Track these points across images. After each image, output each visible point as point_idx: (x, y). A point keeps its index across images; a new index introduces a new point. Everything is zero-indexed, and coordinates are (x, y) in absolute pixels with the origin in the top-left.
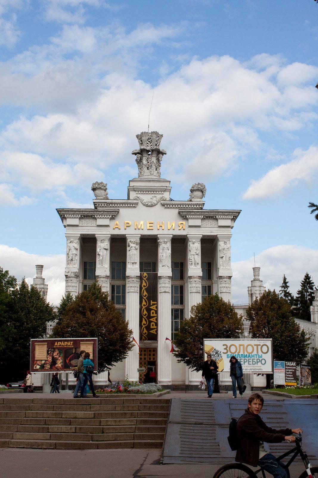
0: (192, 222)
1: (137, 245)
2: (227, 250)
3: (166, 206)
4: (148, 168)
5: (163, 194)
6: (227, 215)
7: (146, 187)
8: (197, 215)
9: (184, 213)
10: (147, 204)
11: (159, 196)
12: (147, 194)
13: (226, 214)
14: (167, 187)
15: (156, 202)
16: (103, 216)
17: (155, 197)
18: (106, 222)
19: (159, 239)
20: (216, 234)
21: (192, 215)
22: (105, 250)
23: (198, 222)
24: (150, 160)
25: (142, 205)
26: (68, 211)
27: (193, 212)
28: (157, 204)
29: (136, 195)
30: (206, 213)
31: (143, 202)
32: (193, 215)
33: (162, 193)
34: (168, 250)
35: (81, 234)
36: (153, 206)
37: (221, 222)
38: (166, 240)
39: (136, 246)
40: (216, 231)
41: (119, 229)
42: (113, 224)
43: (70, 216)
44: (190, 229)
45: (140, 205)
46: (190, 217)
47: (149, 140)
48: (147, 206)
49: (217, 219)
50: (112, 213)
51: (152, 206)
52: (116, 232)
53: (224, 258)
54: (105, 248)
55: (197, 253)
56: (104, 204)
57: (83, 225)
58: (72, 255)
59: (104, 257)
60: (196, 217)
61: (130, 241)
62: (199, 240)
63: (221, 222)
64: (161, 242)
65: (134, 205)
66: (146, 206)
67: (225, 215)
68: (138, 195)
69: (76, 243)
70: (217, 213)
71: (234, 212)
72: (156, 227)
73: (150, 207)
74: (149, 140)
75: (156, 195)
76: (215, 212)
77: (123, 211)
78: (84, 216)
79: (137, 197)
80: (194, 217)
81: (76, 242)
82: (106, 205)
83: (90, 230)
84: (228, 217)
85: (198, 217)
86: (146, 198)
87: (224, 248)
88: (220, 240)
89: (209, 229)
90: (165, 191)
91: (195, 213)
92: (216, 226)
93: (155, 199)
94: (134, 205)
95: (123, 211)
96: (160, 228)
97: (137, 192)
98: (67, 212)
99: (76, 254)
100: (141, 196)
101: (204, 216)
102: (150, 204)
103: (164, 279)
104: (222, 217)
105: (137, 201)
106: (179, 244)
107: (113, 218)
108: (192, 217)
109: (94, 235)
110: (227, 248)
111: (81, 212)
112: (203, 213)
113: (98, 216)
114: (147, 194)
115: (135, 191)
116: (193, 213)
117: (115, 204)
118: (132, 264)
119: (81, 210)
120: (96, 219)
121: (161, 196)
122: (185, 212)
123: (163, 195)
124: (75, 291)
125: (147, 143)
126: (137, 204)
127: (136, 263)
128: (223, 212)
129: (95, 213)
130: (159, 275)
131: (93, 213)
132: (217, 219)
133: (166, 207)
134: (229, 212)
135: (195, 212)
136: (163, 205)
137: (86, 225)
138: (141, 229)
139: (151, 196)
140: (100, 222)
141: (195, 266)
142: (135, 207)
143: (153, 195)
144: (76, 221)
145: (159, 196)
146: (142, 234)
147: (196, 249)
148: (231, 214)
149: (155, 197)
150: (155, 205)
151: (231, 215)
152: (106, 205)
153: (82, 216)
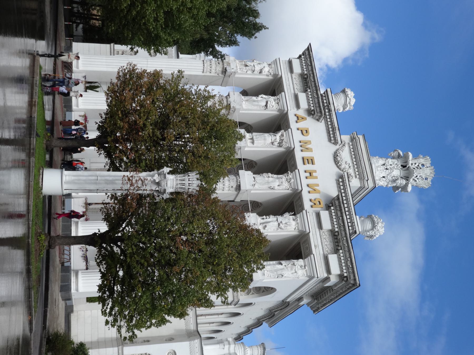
0: (325, 215)
1: (279, 143)
2: (294, 271)
3: (340, 180)
4: (384, 165)
5: (356, 177)
6: (346, 265)
8: (338, 221)
9: (337, 202)
10: (337, 156)
11: (351, 171)
12: (351, 153)
13: (349, 263)
14: (367, 181)
15: (342, 167)
17: (350, 167)
19: (292, 172)
20: (314, 252)
21: (337, 213)
22: (265, 104)
23: (327, 225)
24: (395, 168)
26: (310, 58)
27: (342, 213)
28: (340, 169)
30: (343, 234)
31: (339, 151)
32: (337, 215)
33: (358, 176)
34: (279, 186)
35: (281, 76)
36: (336, 164)
37: (333, 259)
38: (292, 180)
39: (277, 142)
40: (318, 253)
41: (297, 122)
42: (301, 113)
43: (304, 62)
44: (314, 214)
45: (334, 148)
46: (333, 211)
47: (420, 165)
48: (335, 156)
49: (336, 251)
52: (292, 119)
53: (280, 266)
54: (269, 102)
55: (281, 225)
56: (326, 103)
58: (252, 65)
59: (256, 103)
60: (335, 220)
62: (300, 229)
63: (333, 259)
64: (287, 176)
65: (332, 139)
66: (334, 155)
68: (347, 145)
69: (269, 72)
71: (354, 276)
72: (309, 167)
73: (335, 160)
74: (420, 165)
75: (352, 167)
76: (348, 246)
77: (321, 126)
79: (345, 143)
80: (334, 217)
81: (270, 71)
83: (288, 87)
84: (344, 268)
85: (335, 223)
86: (345, 155)
87: (296, 264)
88: (306, 260)
89: (319, 243)
90: (360, 179)
91: (340, 218)
92: (326, 253)
93: (347, 166)
94: (332, 139)
96: (308, 174)
97: (351, 144)
98: (308, 57)
99: (254, 71)
100: (346, 148)
101: (338, 232)
102: (339, 159)
103: (235, 179)
104: (342, 258)
105: (340, 142)
106: (289, 205)
107: (310, 112)
108: (333, 214)
109: (283, 90)
110: (297, 270)
111: (311, 72)
112: (342, 228)
113: (310, 93)
114: (352, 157)
116: (339, 213)
117: (330, 115)
118: (251, 137)
119: (315, 71)
120: (305, 91)
121: (353, 174)
122: (339, 202)
123: (354, 178)
124: (205, 71)
125: (415, 164)
126: (336, 143)
127: (253, 143)
128: (350, 257)
129: (314, 88)
130: (241, 172)
133: (338, 181)
134: (353, 267)
135: (342, 217)
137: (294, 82)
138: (302, 148)
139: (349, 161)
140: (302, 97)
141: (260, 224)
142: (330, 140)
143: (351, 165)
144: (297, 68)
145: (351, 171)
146: (295, 150)
147: (286, 223)
149: (350, 167)
150: (338, 167)
151: (348, 272)
152: (325, 104)
153: (306, 76)
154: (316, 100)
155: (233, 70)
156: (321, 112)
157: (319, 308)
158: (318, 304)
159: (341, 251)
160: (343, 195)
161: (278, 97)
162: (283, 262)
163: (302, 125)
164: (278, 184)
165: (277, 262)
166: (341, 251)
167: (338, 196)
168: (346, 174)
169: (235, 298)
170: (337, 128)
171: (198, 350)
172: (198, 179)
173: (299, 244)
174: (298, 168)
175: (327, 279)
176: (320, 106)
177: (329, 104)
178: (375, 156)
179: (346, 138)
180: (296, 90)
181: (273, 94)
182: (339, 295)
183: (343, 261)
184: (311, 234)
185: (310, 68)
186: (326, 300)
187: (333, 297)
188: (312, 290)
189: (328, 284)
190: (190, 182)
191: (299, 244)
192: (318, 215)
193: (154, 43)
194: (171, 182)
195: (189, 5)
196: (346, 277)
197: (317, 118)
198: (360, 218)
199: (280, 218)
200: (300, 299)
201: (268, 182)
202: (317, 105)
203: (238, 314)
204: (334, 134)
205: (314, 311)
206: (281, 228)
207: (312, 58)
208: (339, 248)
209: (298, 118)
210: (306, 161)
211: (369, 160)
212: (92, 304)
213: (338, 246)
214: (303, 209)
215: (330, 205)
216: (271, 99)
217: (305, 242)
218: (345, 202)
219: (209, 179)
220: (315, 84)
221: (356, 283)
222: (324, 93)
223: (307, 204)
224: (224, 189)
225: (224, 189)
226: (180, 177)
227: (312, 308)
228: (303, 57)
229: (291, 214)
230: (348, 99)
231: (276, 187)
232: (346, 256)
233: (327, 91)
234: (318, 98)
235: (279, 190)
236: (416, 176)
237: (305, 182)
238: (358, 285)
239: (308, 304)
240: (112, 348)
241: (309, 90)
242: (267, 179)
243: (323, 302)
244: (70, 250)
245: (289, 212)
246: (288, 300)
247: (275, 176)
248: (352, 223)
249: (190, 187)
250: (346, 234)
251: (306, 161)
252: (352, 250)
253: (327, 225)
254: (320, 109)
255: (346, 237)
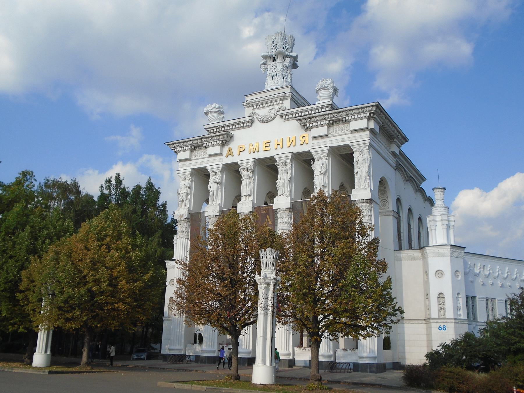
0: (315, 132)
3: (284, 117)
5: (282, 103)
7: (261, 99)
9: (303, 121)
11: (277, 107)
15: (273, 116)
16: (213, 143)
18: (216, 149)
22: (216, 184)
23: (323, 130)
25: (258, 122)
27: (313, 117)
29: (251, 111)
38: (283, 161)
45: (257, 123)
50: (221, 137)
51: (269, 120)
52: (230, 160)
57: (196, 158)
61: (243, 169)
62: (326, 155)
65: (248, 124)
67: (355, 113)
70: (345, 113)
71: (369, 107)
72: (273, 145)
74: (274, 45)
75: (273, 107)
78: (195, 147)
82: (218, 130)
84: (362, 116)
86: (263, 112)
89: (340, 137)
92: (349, 132)
93: (273, 111)
95: (236, 133)
97: (252, 108)
98: (176, 145)
100: (257, 111)
102: (265, 119)
104: (353, 117)
105: (251, 118)
107: (224, 144)
111: (189, 143)
112: (326, 117)
115: (250, 106)
117: (227, 126)
121: (279, 106)
122: (303, 119)
123: (283, 105)
126: (252, 122)
129: (203, 140)
131: (200, 141)
132: (347, 122)
133: (285, 119)
135: (316, 117)
136: (281, 116)
137: (198, 157)
139: (268, 109)
140: (212, 150)
143: (271, 107)
148: (364, 110)
150: (273, 119)
153: (193, 147)
154: (213, 138)
155: (187, 212)
156: (224, 134)
157: (403, 137)
158: (398, 139)
159: (347, 118)
160: (297, 115)
161: (210, 172)
162: (356, 171)
163: (236, 151)
164: (286, 174)
165: (355, 176)
166: (347, 118)
167: (297, 120)
168: (278, 113)
169: (390, 214)
170: (239, 120)
171: (436, 249)
172: (265, 251)
173: (341, 156)
174: (272, 155)
175: (372, 131)
176: (219, 135)
177: (217, 126)
178: (265, 85)
179: (248, 111)
180: (205, 156)
181: (208, 176)
182: (388, 119)
183: (356, 117)
184: (331, 145)
185: (185, 144)
186: (394, 132)
187: (390, 125)
188: (384, 144)
189: (377, 130)
190: (268, 257)
191: (341, 156)
192: (314, 138)
193: (160, 282)
194: (268, 273)
195: (124, 252)
196: (370, 114)
197: (229, 138)
198: (318, 100)
199: (316, 173)
200: (394, 154)
201: (283, 183)
202: (218, 138)
203: (410, 210)
204: (243, 123)
205: (406, 141)
206: (326, 172)
207: (177, 142)
208: (344, 119)
209: (230, 154)
210: (267, 149)
211: (267, 91)
212: (392, 345)
213: (342, 120)
214: (309, 152)
215: (306, 127)
216: (212, 178)
217: (339, 151)
218: (303, 114)
219: (270, 240)
220: (199, 139)
221: (376, 105)
222: (208, 131)
223: (305, 148)
224: (284, 225)
225: (284, 225)
226: (263, 266)
227: (403, 144)
228: (176, 150)
229: (312, 163)
230: (213, 110)
231: (289, 175)
232: (351, 114)
233: (206, 129)
234: (211, 137)
235: (291, 173)
236: (284, 48)
237: (286, 150)
238: (377, 103)
239: (399, 147)
240: (432, 329)
241: (205, 145)
242: (281, 184)
243: (396, 134)
244: (340, 363)
245: (311, 165)
246: (395, 165)
247: (279, 176)
248: (322, 107)
249: (272, 257)
250: (331, 114)
251: (267, 149)
252: (346, 109)
253: (323, 130)
254: (221, 135)
255: (334, 113)
